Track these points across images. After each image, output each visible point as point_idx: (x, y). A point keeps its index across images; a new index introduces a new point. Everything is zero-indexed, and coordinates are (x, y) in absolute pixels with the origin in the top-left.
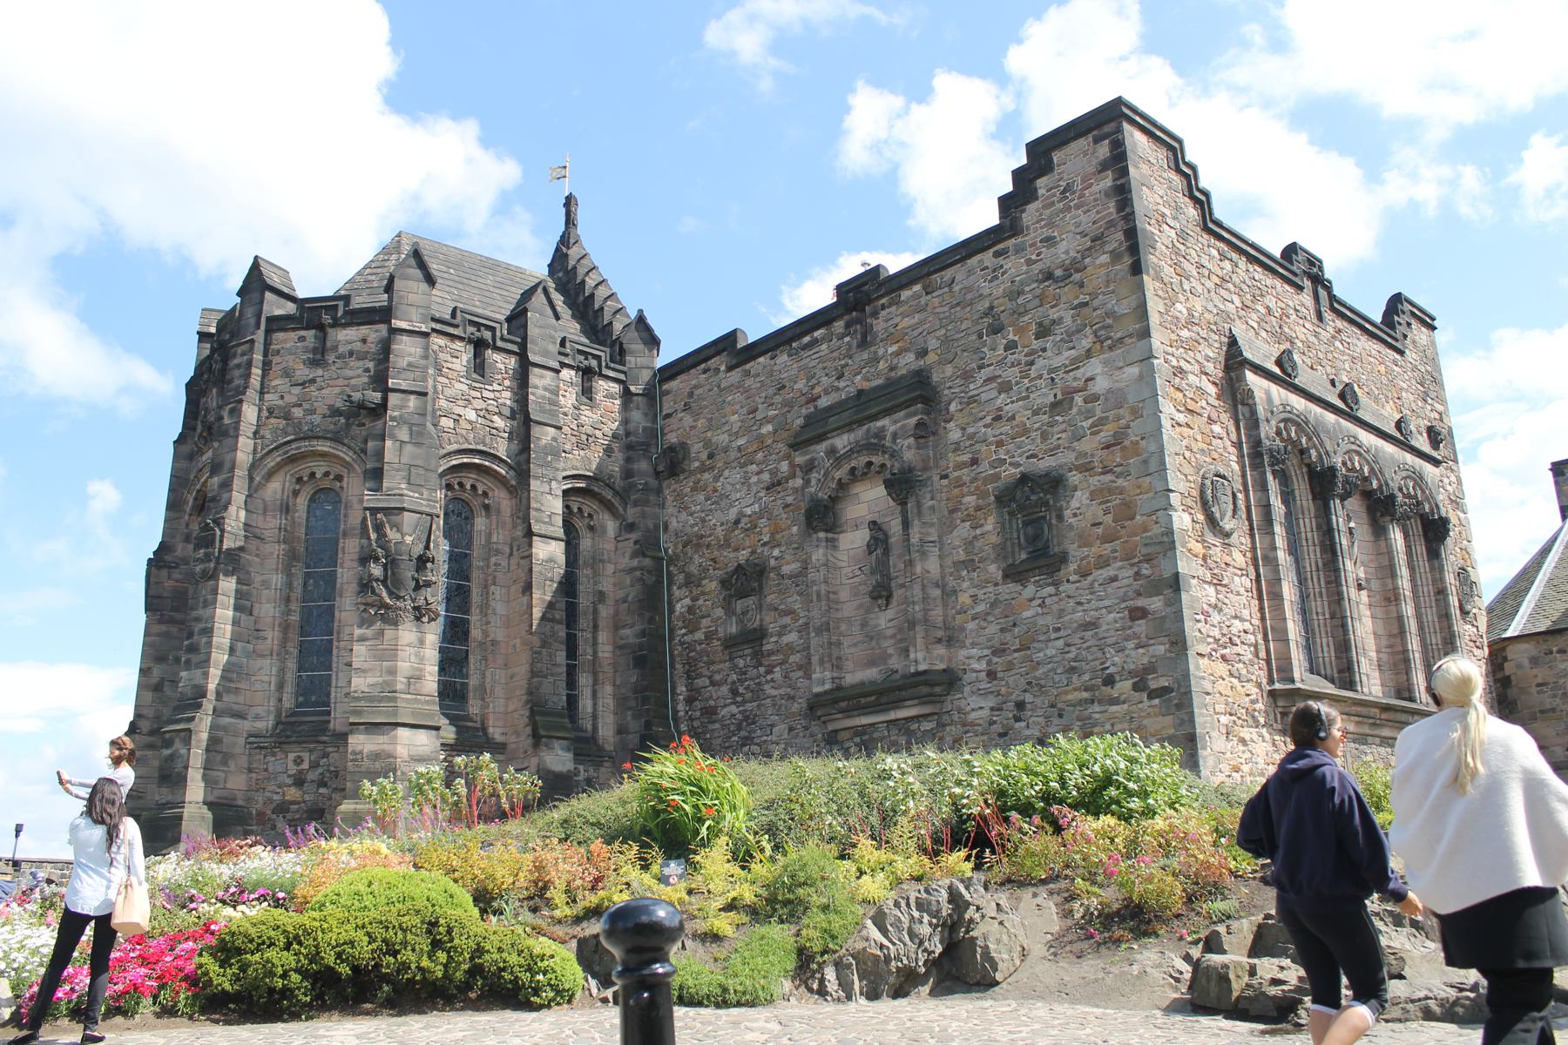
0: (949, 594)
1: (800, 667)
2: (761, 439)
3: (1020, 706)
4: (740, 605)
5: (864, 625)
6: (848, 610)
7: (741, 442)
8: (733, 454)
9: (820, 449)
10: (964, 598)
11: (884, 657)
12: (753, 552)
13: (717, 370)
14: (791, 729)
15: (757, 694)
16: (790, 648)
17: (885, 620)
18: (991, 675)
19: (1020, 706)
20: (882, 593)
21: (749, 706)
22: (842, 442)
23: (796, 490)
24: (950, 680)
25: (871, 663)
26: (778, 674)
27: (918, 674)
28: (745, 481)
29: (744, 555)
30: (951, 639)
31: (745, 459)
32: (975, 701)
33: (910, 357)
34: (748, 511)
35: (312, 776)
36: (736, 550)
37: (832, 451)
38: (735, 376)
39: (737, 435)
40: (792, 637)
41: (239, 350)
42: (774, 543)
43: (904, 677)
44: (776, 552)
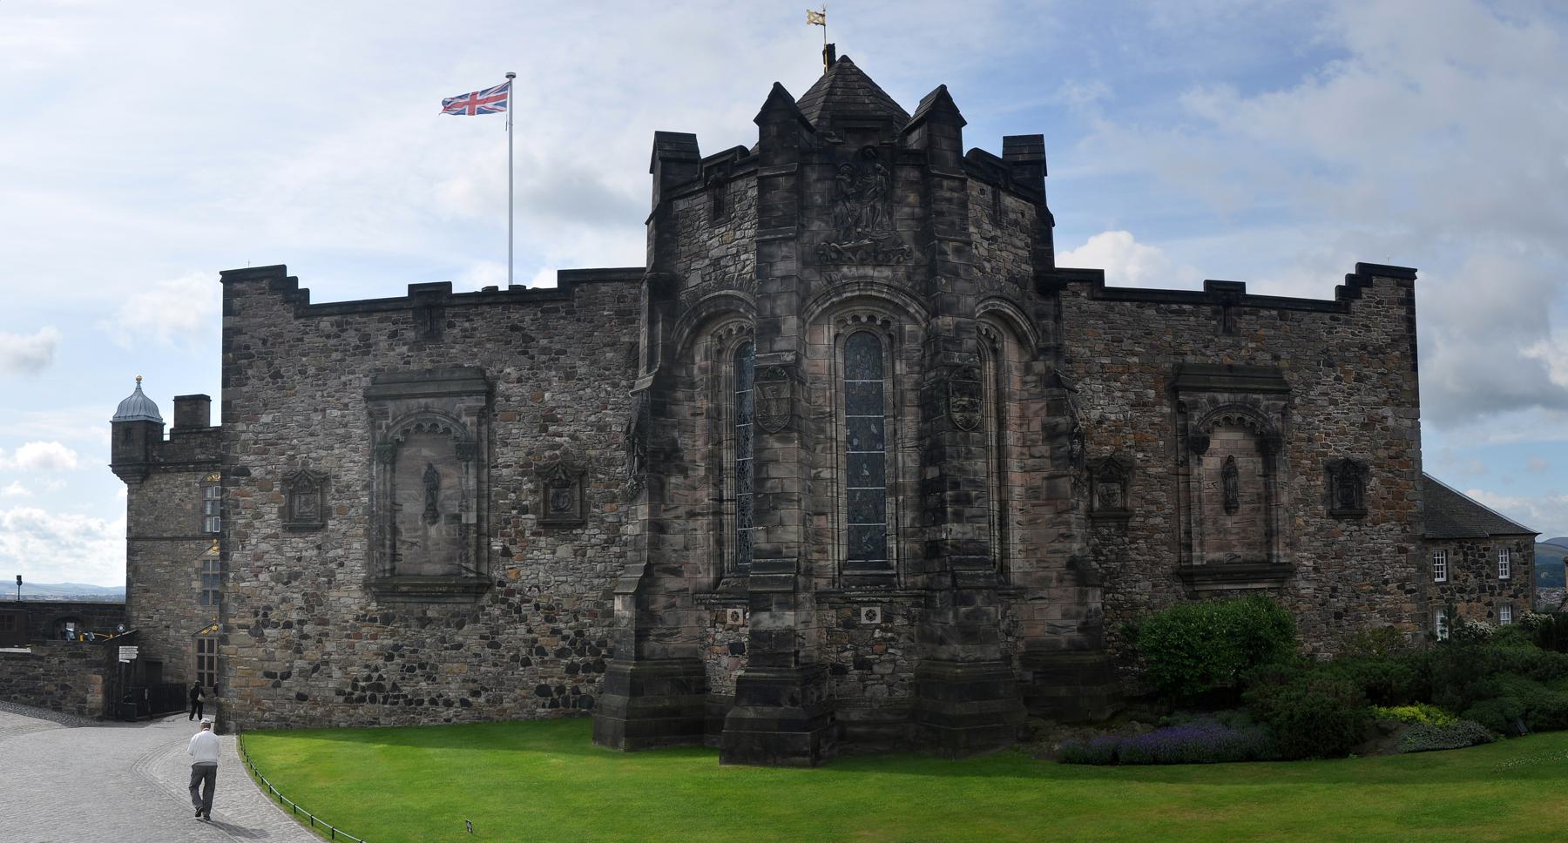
0: (1292, 517)
1: (1164, 544)
2: (1128, 368)
3: (1334, 589)
4: (1101, 487)
5: (1215, 523)
6: (1207, 509)
7: (1105, 361)
8: (1097, 368)
9: (1204, 398)
10: (1300, 521)
11: (1229, 546)
12: (1118, 450)
13: (1076, 294)
14: (1154, 586)
15: (1121, 556)
16: (1155, 528)
17: (1229, 522)
18: (1316, 569)
19: (1334, 589)
20: (1230, 506)
21: (1113, 565)
22: (1223, 398)
23: (1163, 415)
24: (1289, 570)
25: (1220, 548)
26: (1142, 544)
27: (1279, 564)
28: (1109, 392)
29: (1107, 450)
30: (1292, 545)
31: (1108, 376)
32: (1302, 584)
33: (1268, 356)
34: (1113, 417)
35: (1002, 627)
36: (1100, 444)
37: (1214, 401)
38: (1096, 306)
39: (1101, 354)
40: (1159, 520)
41: (945, 183)
42: (1138, 447)
43: (1246, 562)
44: (1140, 455)
